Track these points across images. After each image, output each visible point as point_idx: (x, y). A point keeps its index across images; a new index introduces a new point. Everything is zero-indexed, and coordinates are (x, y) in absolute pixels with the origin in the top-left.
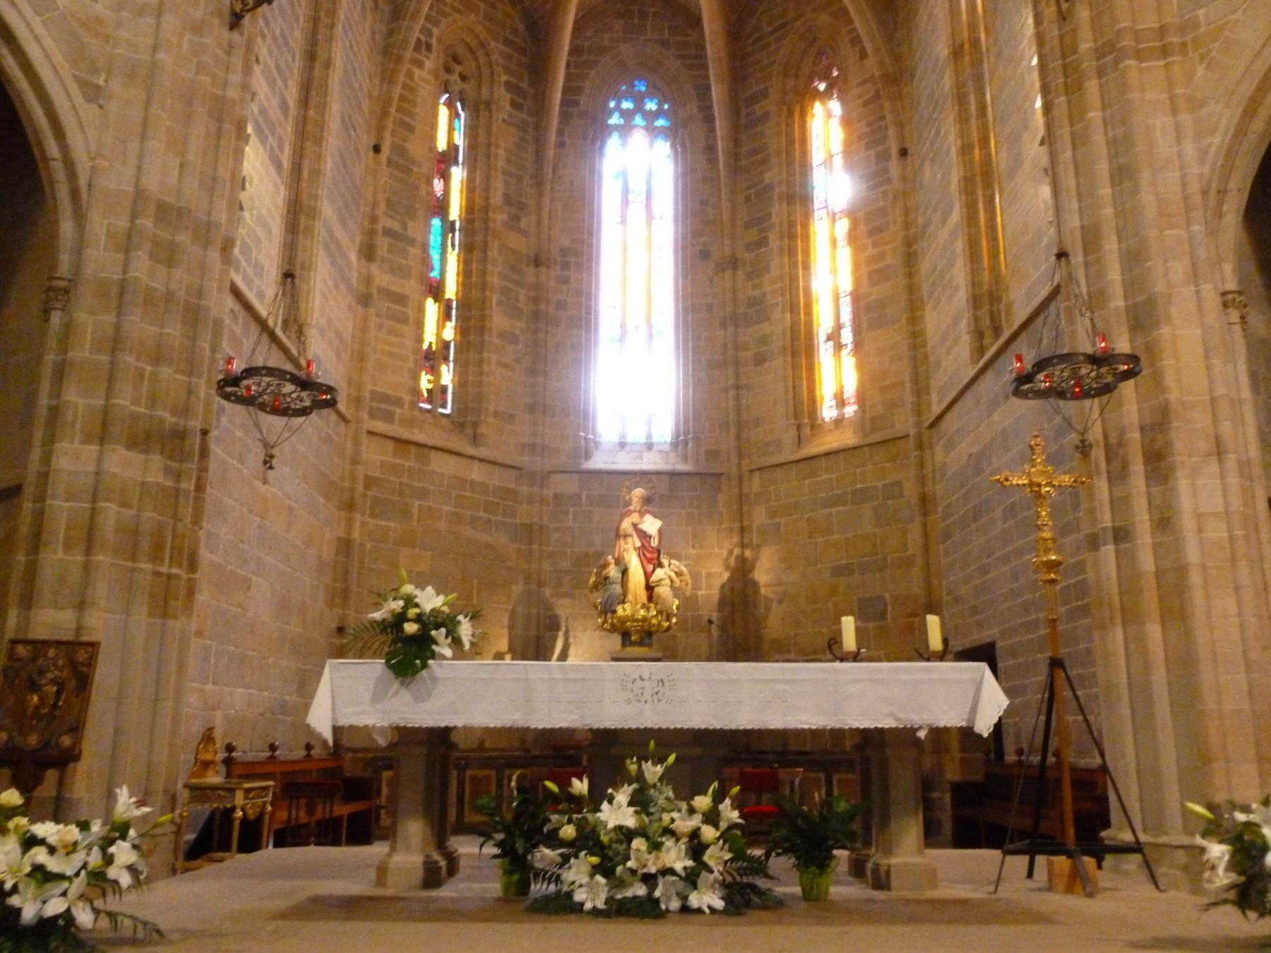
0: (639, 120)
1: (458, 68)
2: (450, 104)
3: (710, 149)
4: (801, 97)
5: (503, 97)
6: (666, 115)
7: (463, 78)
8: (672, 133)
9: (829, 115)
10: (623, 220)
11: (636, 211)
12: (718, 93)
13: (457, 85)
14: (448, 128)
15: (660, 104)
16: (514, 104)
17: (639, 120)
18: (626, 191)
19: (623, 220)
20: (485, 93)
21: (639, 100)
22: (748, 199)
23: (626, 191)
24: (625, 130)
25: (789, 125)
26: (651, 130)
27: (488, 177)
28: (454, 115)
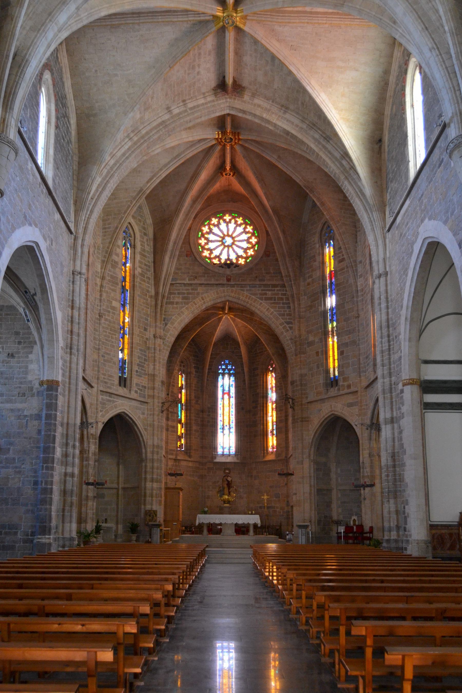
0: (227, 371)
1: (183, 364)
2: (181, 374)
3: (244, 381)
4: (266, 372)
5: (193, 370)
6: (234, 370)
7: (184, 366)
8: (234, 375)
9: (272, 376)
10: (223, 398)
11: (226, 396)
12: (246, 370)
13: (182, 368)
14: (181, 381)
15: (232, 367)
16: (196, 372)
17: (227, 371)
18: (224, 390)
19: (223, 398)
20: (189, 370)
21: (226, 365)
22: (253, 395)
23: (224, 390)
24: (223, 375)
25: (263, 378)
26: (230, 375)
27: (190, 392)
28: (182, 377)
